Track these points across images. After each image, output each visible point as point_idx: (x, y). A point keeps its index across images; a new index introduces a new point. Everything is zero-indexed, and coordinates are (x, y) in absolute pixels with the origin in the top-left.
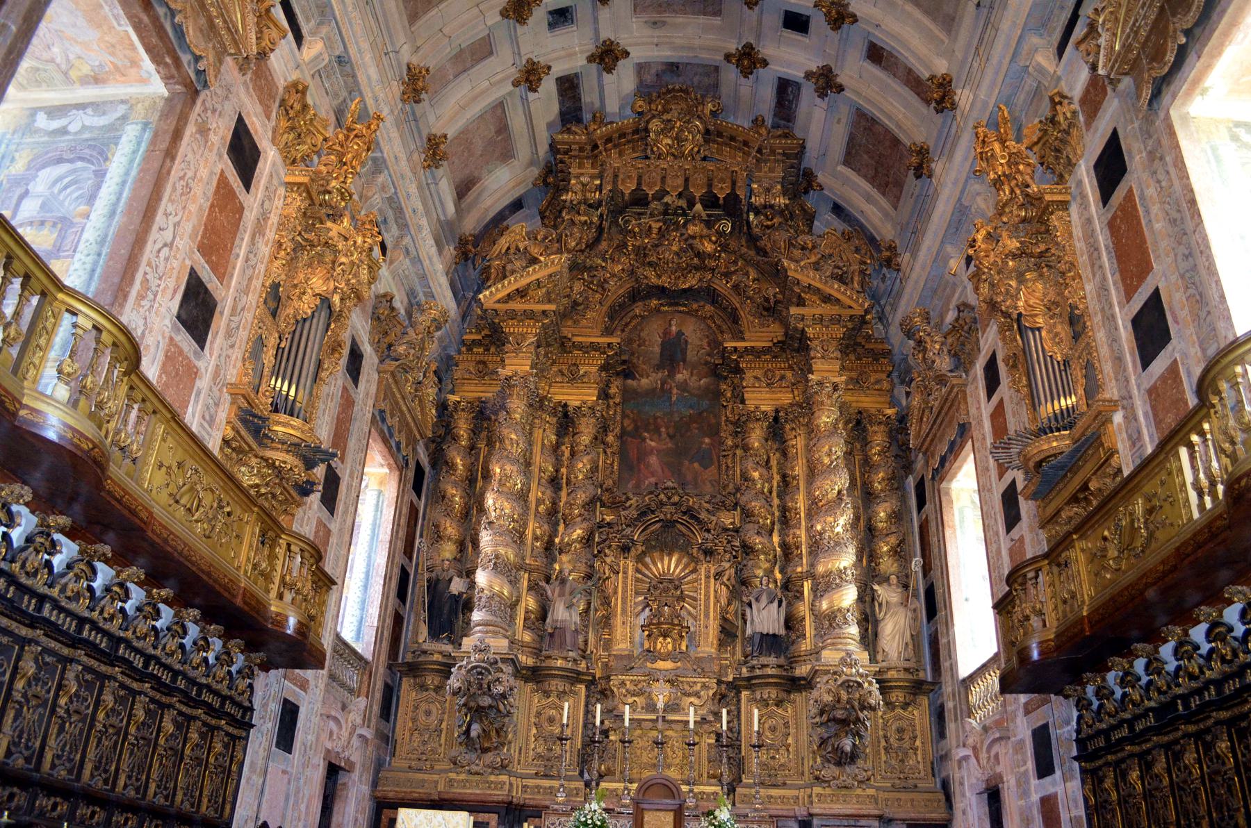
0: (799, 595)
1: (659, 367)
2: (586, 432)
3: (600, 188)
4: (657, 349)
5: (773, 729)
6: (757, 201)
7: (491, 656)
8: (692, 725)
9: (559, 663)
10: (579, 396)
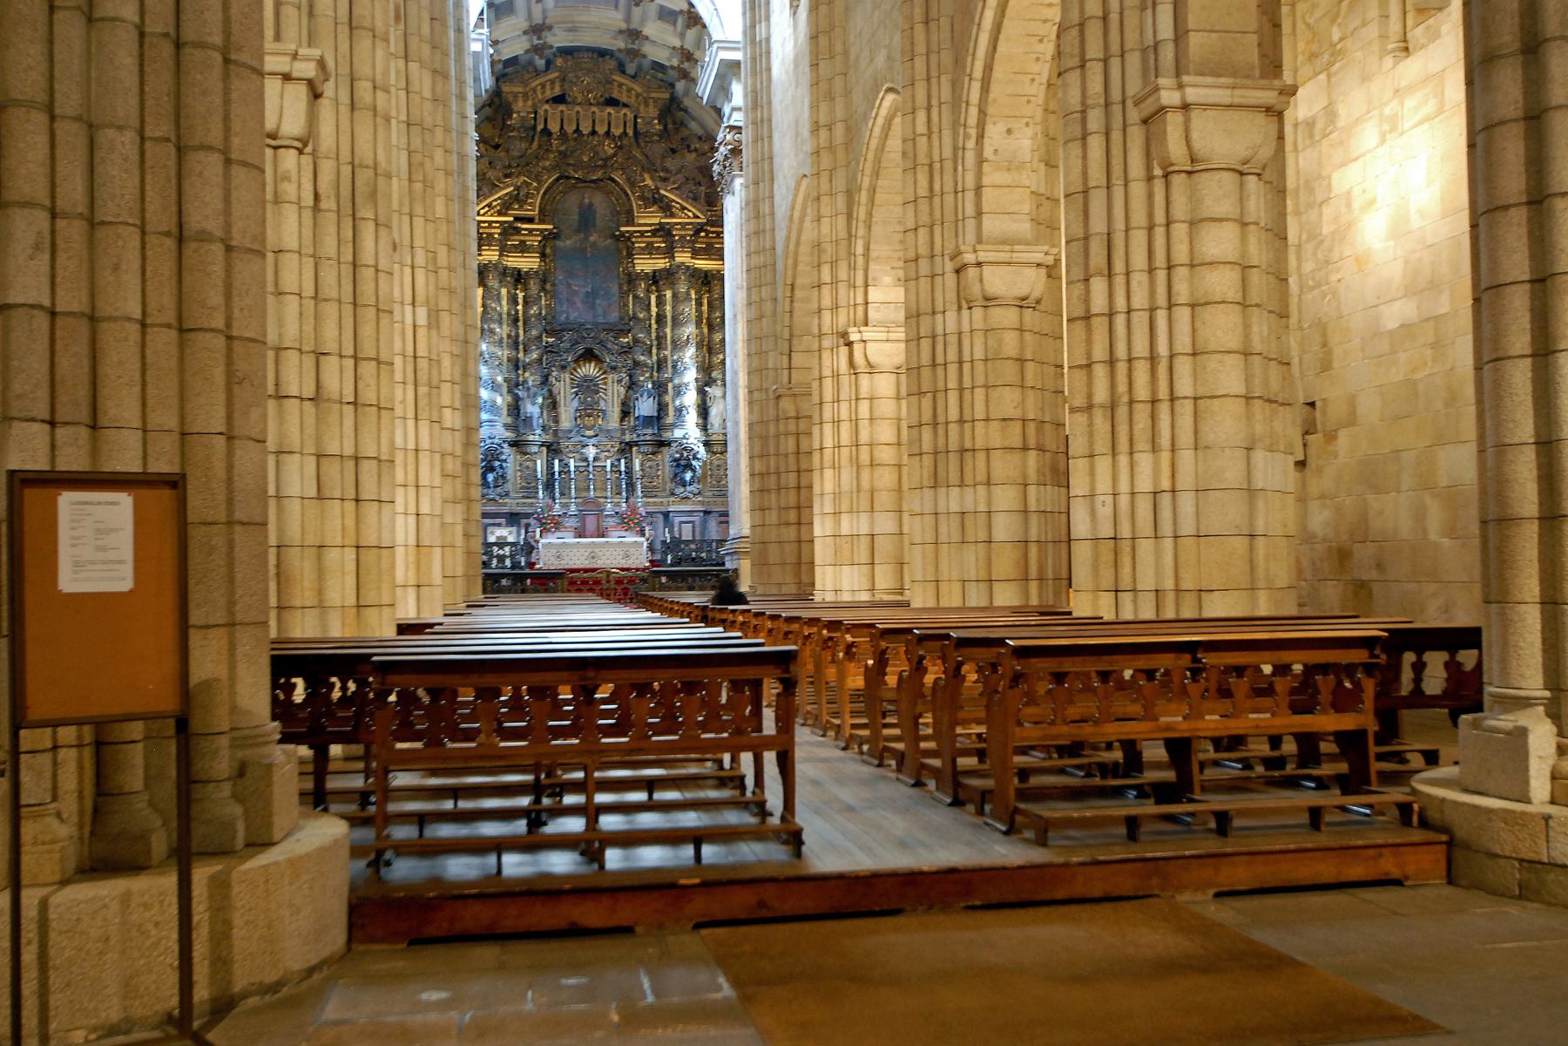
0: (666, 392)
1: (578, 231)
2: (534, 286)
3: (535, 119)
4: (576, 217)
5: (650, 467)
6: (642, 128)
7: (496, 441)
8: (608, 469)
9: (531, 438)
10: (528, 263)
